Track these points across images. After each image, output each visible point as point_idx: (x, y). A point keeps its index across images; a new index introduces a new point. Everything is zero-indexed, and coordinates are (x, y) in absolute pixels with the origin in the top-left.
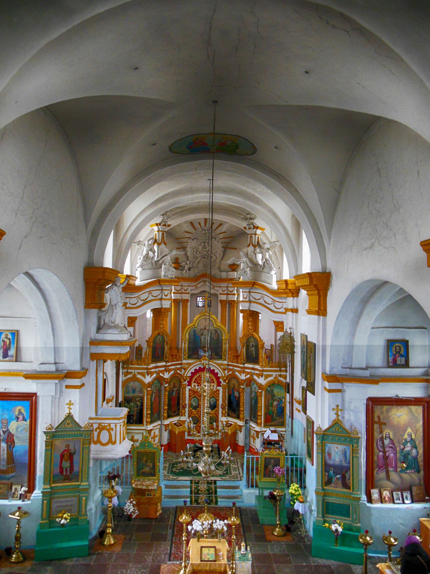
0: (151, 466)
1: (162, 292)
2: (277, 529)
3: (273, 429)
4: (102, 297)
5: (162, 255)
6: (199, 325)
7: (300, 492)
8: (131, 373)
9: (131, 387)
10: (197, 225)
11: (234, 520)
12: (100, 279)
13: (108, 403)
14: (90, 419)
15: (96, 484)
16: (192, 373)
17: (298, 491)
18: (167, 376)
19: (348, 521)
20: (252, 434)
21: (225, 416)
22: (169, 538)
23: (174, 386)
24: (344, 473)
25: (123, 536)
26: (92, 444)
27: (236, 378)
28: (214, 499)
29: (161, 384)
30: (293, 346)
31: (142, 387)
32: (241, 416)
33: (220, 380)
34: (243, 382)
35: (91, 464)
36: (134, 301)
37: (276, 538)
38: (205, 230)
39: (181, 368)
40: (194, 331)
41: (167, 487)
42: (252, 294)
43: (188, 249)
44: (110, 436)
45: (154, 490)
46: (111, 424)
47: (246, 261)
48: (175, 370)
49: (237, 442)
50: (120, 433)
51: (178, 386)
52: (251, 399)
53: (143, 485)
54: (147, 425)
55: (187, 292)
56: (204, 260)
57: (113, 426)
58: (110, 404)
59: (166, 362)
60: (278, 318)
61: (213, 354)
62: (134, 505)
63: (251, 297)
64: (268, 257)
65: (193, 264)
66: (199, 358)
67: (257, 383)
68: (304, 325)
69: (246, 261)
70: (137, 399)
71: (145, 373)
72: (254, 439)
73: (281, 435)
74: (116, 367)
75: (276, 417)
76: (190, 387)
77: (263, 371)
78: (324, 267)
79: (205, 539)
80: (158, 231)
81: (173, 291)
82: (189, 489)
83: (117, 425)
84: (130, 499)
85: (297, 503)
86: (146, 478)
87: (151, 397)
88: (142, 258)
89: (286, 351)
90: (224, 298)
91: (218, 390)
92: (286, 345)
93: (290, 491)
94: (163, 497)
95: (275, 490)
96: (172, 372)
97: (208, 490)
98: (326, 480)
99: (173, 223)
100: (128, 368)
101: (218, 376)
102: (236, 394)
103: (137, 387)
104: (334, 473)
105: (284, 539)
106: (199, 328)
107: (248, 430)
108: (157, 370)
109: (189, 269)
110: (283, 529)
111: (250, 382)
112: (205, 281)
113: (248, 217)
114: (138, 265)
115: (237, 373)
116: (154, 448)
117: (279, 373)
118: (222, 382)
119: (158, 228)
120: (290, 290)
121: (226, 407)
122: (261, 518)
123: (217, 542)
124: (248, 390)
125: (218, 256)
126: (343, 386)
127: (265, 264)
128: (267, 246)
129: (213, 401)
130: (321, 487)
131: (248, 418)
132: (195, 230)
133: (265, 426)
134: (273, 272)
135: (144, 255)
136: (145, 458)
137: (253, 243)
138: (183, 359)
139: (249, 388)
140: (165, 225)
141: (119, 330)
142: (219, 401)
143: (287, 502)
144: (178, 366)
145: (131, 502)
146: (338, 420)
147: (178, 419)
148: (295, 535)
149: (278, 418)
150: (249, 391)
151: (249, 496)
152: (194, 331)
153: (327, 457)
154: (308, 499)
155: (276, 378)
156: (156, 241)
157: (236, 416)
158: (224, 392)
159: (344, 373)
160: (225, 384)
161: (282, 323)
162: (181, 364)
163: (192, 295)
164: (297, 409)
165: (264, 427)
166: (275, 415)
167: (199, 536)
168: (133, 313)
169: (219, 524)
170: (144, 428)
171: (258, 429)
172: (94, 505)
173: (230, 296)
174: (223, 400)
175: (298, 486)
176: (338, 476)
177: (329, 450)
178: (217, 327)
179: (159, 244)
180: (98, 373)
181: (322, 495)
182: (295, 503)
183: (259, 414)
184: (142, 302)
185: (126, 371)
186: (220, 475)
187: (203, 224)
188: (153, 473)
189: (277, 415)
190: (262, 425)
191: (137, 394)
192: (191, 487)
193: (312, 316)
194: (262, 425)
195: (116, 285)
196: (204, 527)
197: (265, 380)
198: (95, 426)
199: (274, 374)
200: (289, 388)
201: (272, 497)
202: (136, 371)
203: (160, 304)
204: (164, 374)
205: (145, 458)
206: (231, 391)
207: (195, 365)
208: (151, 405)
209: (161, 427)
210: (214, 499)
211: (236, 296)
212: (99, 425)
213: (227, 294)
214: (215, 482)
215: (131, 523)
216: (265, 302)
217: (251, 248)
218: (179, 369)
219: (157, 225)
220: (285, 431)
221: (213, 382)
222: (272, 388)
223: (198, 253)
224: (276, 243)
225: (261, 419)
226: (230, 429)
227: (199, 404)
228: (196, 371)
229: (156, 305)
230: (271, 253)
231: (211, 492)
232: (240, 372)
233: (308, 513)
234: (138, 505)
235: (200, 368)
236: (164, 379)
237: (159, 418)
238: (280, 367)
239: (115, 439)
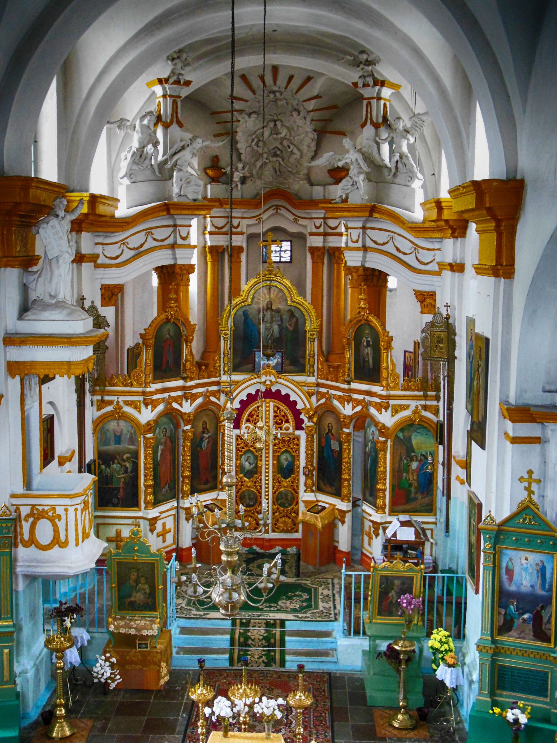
0: (148, 591)
1: (174, 231)
2: (400, 717)
3: (404, 517)
4: (28, 242)
5: (173, 150)
6: (256, 300)
7: (452, 645)
8: (110, 403)
9: (112, 432)
10: (256, 83)
11: (300, 698)
12: (18, 204)
13: (61, 464)
14: (13, 496)
15: (35, 624)
17: (447, 643)
18: (187, 408)
19: (541, 703)
20: (366, 528)
21: (312, 491)
22: (180, 728)
23: (205, 429)
24: (539, 609)
25: (90, 723)
26: (20, 546)
27: (333, 411)
28: (278, 657)
29: (177, 426)
30: (452, 345)
31: (135, 432)
32: (345, 491)
33: (302, 416)
34: (347, 421)
35: (21, 585)
36: (113, 251)
37: (395, 732)
38: (274, 92)
39: (219, 391)
40: (245, 314)
41: (184, 631)
42: (369, 232)
43: (239, 137)
44: (56, 531)
45: (153, 636)
46: (57, 508)
47: (357, 160)
48: (206, 395)
49: (336, 544)
50: (76, 525)
51: (212, 430)
52: (366, 455)
53: (131, 628)
54: (146, 508)
55: (239, 230)
56: (275, 159)
57: (60, 511)
58: (67, 465)
59: (184, 379)
60: (425, 283)
61: (287, 362)
62: (112, 666)
63: (368, 239)
64: (405, 149)
65: (250, 171)
66: (254, 370)
67: (376, 424)
68: (472, 300)
69: (357, 160)
70: (125, 457)
71: (139, 401)
72: (370, 538)
73: (424, 530)
74: (77, 391)
75: (416, 493)
77: (388, 397)
78: (512, 168)
79: (243, 734)
80: (164, 96)
81: (209, 229)
82: (228, 637)
83: (69, 508)
84: (104, 653)
85: (442, 667)
86: (138, 614)
87: (155, 451)
88: (129, 156)
89: (437, 354)
90: (317, 242)
91: (298, 438)
92: (439, 342)
93: (430, 643)
94: (174, 650)
95: (396, 640)
96: (200, 400)
97: (266, 638)
98: (501, 623)
99: (199, 77)
100: (103, 393)
101: (298, 407)
102: (335, 446)
103: (125, 432)
104: (517, 609)
105: (412, 734)
106: (255, 306)
107: (358, 521)
108: (166, 395)
109: (243, 180)
110: (411, 717)
111: (361, 421)
112: (277, 207)
113: (361, 58)
114: (123, 172)
115: (336, 403)
116: (152, 555)
117: (423, 402)
118: (306, 420)
119: (164, 89)
120: (447, 221)
121: (314, 473)
122: (369, 692)
123: (262, 739)
124: (359, 437)
125: (305, 148)
126: (544, 429)
127: (400, 165)
128: (405, 122)
129: (286, 460)
130: (489, 638)
131: (361, 497)
132: (254, 92)
133: (393, 512)
134: (417, 185)
135: (134, 149)
136: (134, 576)
137: (374, 119)
138: (222, 372)
139: (361, 434)
140: (177, 82)
141: (65, 312)
142: (298, 460)
143: (424, 664)
144: (211, 388)
145: (107, 660)
146: (531, 501)
147: (215, 497)
148: (435, 728)
149: (419, 496)
150: (361, 440)
151: (349, 653)
152: (245, 314)
153: (505, 577)
154: (468, 660)
155: (416, 412)
156: (159, 118)
157: (334, 492)
158: (309, 442)
159: (548, 402)
160: (311, 424)
161: (432, 295)
162: (218, 383)
163: (252, 237)
164: (458, 478)
165: (390, 515)
166: (413, 489)
167: (226, 727)
168: (113, 277)
169: (268, 706)
170: (140, 514)
171: (377, 517)
172: (32, 663)
173: (330, 238)
174: (307, 458)
175: (447, 633)
176: (526, 616)
177: (510, 564)
178: (293, 304)
179: (166, 126)
180: (28, 402)
181: (491, 652)
182: (438, 666)
183: (380, 486)
184: (133, 253)
185: (99, 398)
186: (294, 610)
187: (269, 78)
188: (150, 604)
189: (418, 490)
190: (387, 510)
191: (125, 446)
192: (232, 633)
193: (485, 277)
194: (387, 510)
195: (57, 216)
196: (235, 710)
197: (393, 416)
198: (25, 511)
199: (413, 404)
200: (442, 433)
201: (392, 654)
202: (121, 398)
203: (171, 256)
204: (181, 405)
205: (134, 576)
206: (323, 440)
207: (247, 385)
208: (155, 469)
209: (178, 512)
210: (278, 657)
211: (344, 238)
212: (32, 509)
213: (325, 234)
214: (282, 622)
215: (109, 698)
216: (398, 249)
217: (369, 130)
218: (214, 394)
219: (160, 81)
220: (435, 523)
221: (287, 421)
222: (406, 433)
223: (261, 144)
224: (424, 118)
225: (384, 496)
226: (321, 518)
227: (256, 466)
228: (252, 398)
229: (163, 258)
230: (412, 140)
231: (274, 642)
232: (341, 399)
233: (466, 688)
234: (121, 666)
236: (182, 414)
237: (174, 493)
238: (425, 389)
239: (67, 536)
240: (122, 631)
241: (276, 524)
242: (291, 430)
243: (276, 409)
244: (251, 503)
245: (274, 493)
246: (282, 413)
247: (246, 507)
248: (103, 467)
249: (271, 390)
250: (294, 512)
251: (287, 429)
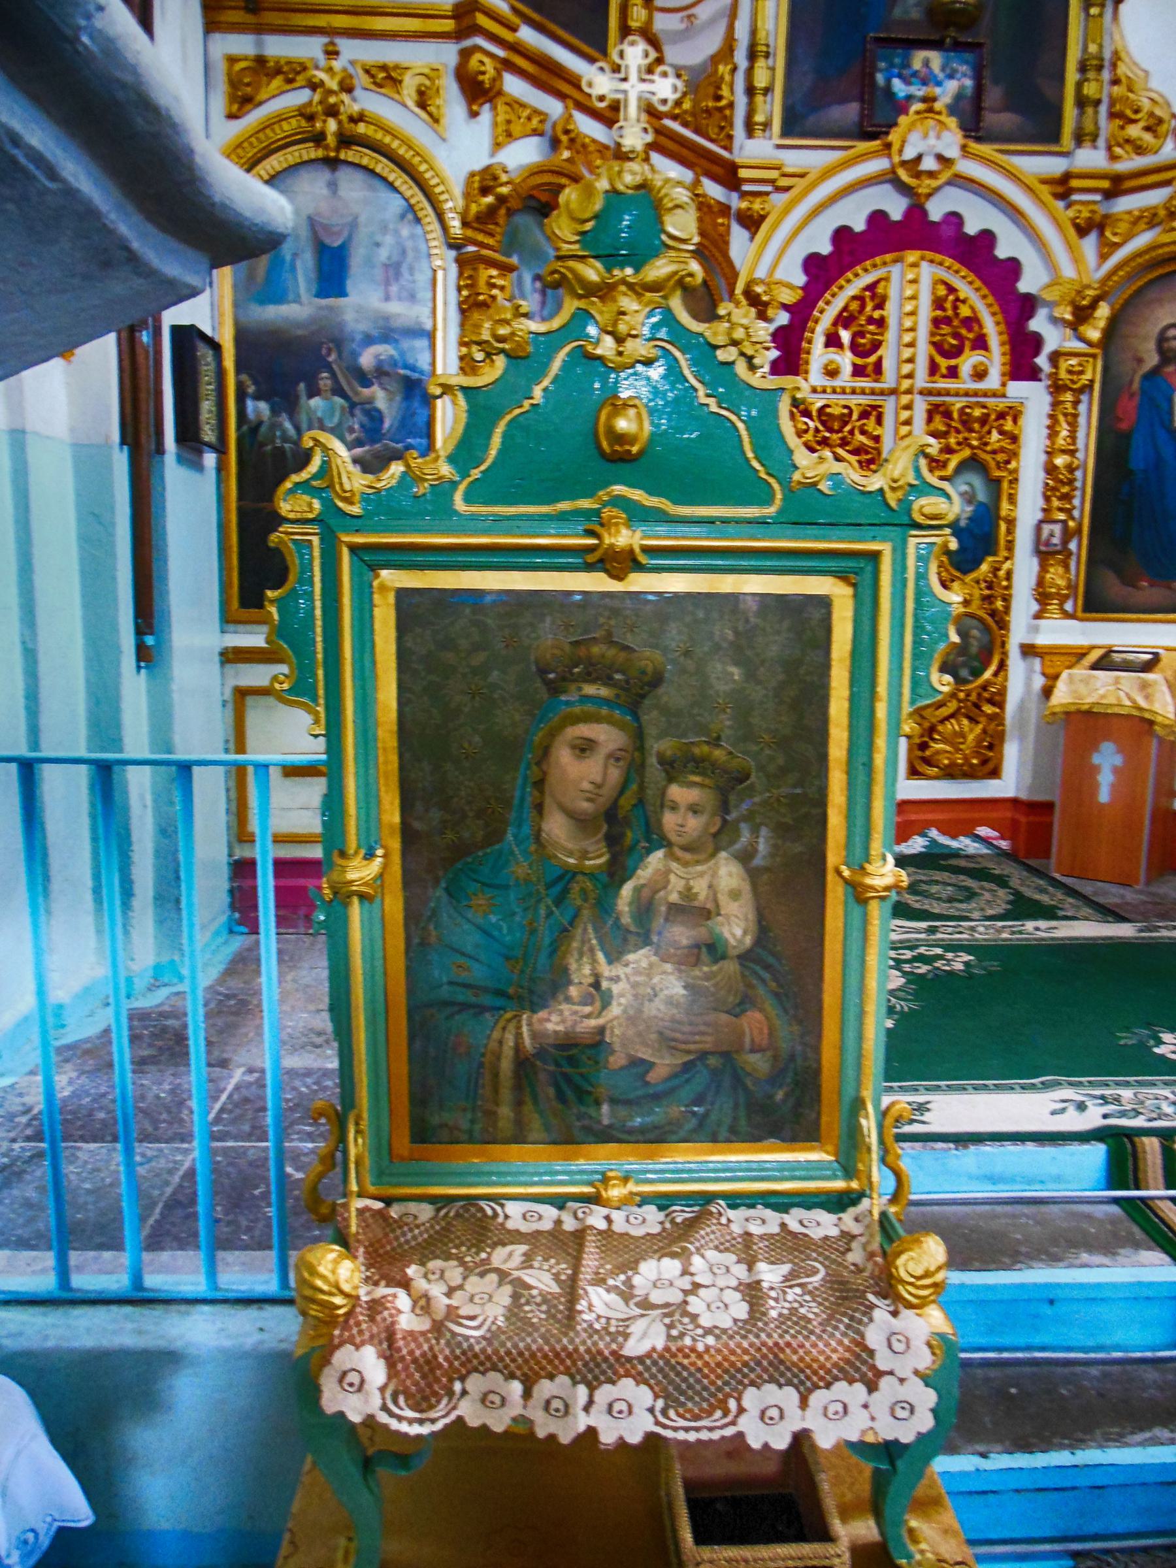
16: (812, 263)
33: (1038, 324)
61: (994, 95)
101: (1024, 286)
221: (981, 343)
228: (850, 248)
235: (878, 218)
240: (487, 1405)
241: (923, 746)
242: (993, 381)
243: (942, 291)
246: (965, 311)
248: (258, 409)
249: (924, 213)
250: (991, 702)
251: (980, 374)
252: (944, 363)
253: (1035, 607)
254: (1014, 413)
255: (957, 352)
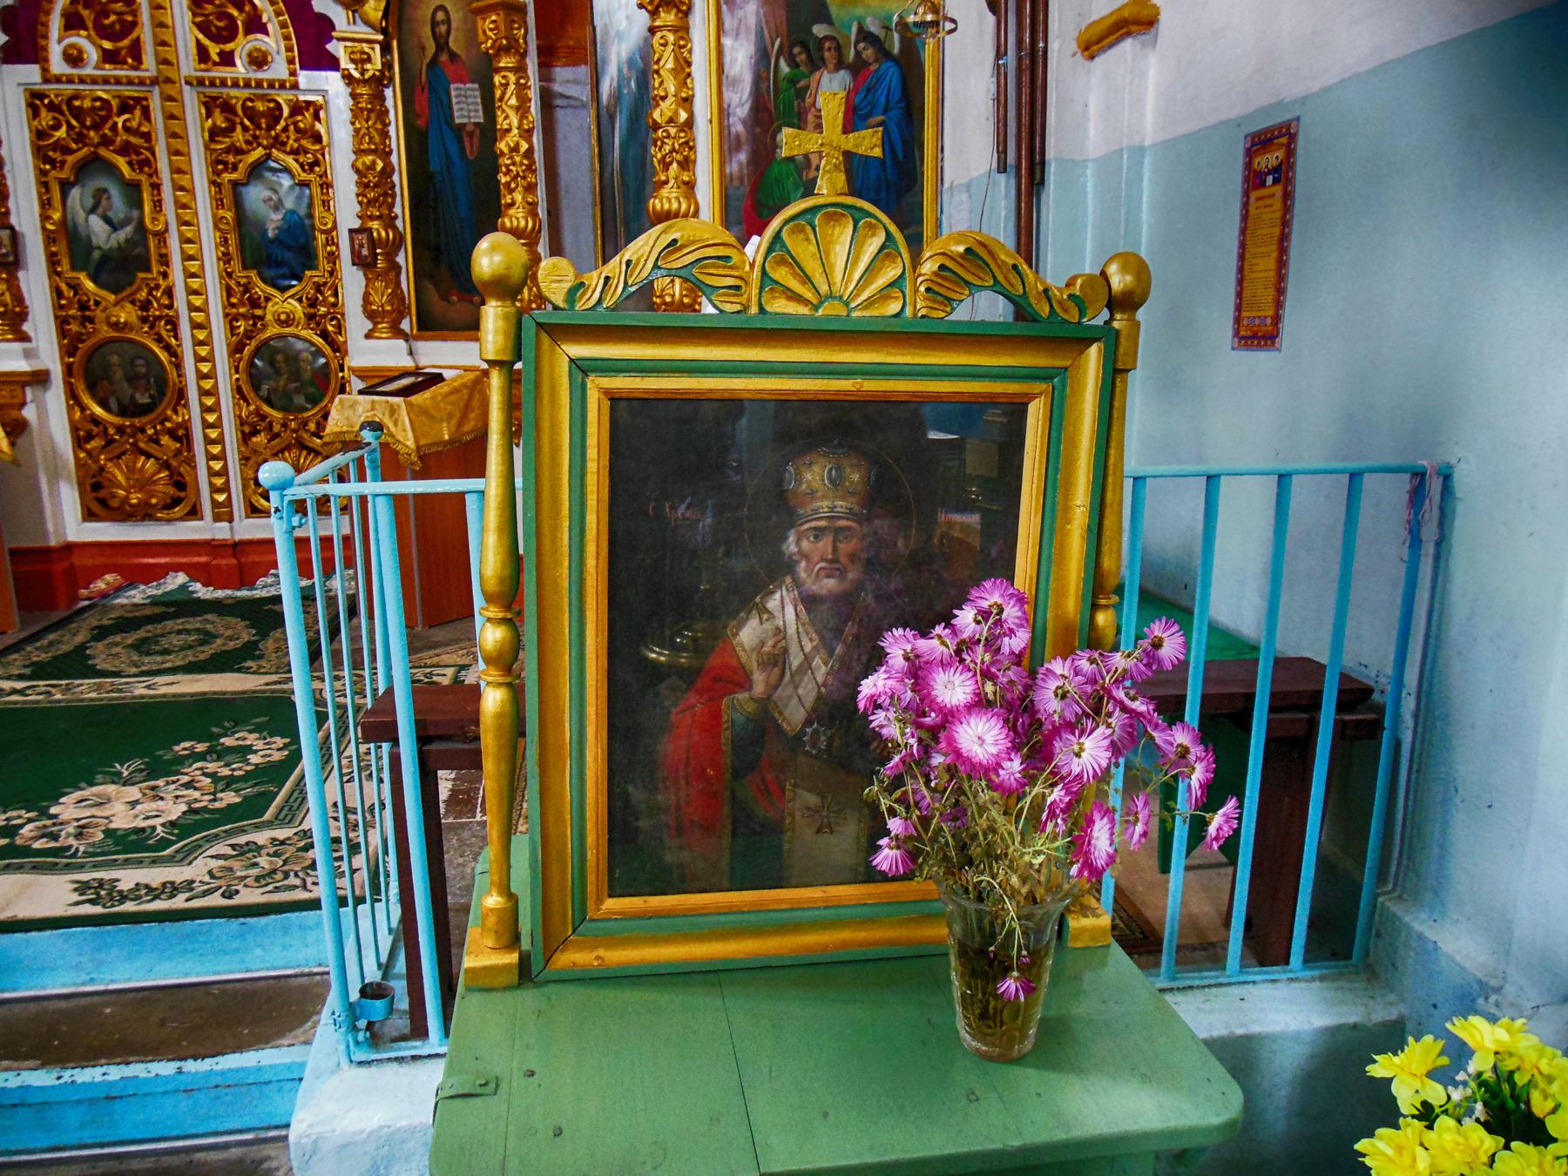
21: (398, 333)
76: (30, 73)
121: (400, 259)
160: (362, 31)
244: (144, 399)
245: (236, 349)
247: (122, 413)
252: (214, 50)
253: (370, 325)
254: (316, 110)
255: (228, 34)
